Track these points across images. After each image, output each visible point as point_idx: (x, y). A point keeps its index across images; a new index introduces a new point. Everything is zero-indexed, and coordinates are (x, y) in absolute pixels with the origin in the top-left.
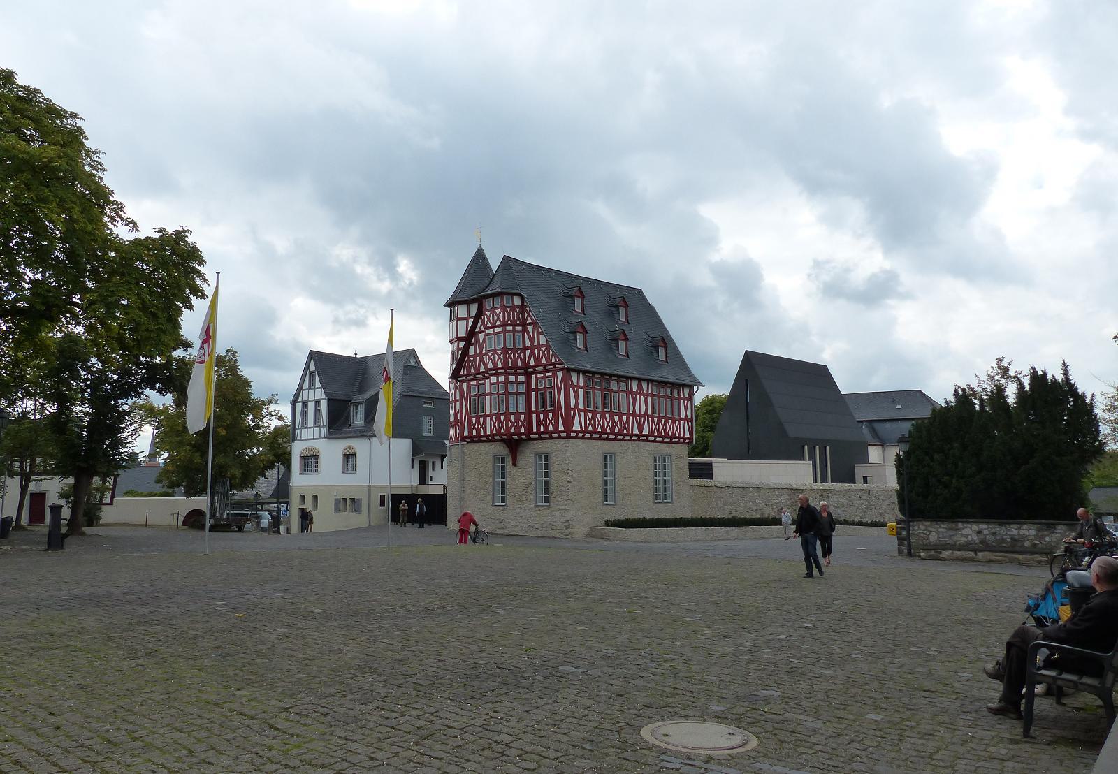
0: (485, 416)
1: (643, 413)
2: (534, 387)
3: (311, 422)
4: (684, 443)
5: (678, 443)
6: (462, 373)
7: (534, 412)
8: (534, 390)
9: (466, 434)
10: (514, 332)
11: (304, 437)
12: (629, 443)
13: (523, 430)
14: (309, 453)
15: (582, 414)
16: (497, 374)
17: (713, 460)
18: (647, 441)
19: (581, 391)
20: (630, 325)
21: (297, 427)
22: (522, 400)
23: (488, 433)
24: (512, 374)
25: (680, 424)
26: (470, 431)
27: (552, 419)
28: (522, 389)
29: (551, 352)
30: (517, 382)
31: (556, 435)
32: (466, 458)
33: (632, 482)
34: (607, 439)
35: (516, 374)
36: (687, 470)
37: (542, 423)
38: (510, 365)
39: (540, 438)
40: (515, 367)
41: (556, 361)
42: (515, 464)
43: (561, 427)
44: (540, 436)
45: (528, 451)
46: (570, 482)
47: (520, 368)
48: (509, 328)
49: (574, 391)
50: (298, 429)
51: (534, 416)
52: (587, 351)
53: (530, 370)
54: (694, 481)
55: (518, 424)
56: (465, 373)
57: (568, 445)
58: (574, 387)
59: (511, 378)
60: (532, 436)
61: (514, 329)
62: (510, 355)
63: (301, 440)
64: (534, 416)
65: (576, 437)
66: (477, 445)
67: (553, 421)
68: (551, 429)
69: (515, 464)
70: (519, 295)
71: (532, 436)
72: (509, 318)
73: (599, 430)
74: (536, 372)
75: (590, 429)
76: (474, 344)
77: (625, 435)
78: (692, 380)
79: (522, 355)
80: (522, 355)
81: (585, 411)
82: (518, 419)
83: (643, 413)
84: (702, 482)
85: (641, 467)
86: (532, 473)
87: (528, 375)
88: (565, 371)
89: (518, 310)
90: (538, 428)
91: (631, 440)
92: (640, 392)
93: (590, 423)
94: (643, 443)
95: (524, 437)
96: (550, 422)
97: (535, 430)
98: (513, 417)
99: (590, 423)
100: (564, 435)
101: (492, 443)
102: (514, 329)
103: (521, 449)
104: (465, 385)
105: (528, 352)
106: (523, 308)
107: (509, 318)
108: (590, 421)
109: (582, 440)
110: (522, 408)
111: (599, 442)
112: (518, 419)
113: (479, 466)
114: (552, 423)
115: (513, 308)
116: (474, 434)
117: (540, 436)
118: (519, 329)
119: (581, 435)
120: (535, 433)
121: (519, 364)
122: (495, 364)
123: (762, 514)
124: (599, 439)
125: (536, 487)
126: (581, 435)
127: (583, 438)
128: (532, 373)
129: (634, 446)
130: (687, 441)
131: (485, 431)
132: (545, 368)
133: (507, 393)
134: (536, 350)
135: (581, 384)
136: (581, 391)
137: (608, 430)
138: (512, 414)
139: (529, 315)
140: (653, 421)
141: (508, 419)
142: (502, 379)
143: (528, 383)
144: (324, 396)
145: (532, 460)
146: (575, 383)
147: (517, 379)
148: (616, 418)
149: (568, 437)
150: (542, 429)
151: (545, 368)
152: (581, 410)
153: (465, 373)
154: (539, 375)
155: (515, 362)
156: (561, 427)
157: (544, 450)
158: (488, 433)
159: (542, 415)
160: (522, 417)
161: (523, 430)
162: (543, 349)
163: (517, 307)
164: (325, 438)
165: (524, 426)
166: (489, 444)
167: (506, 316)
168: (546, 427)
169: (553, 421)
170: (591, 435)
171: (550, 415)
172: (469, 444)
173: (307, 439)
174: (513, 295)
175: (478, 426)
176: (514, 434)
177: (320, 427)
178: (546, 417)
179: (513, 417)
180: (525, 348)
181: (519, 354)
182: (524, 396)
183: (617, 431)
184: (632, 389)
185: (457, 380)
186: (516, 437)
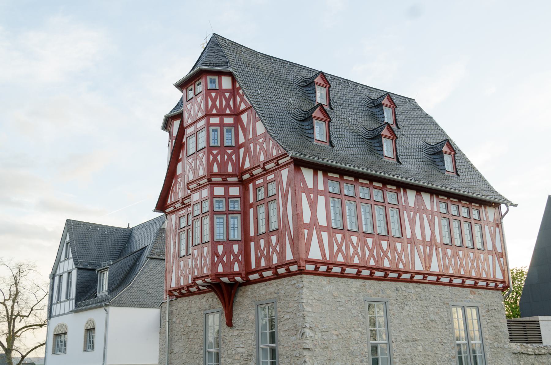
1: (428, 239)
2: (251, 201)
3: (63, 297)
4: (496, 288)
5: (486, 288)
6: (169, 202)
8: (251, 206)
10: (222, 125)
11: (58, 313)
12: (410, 285)
13: (236, 268)
14: (60, 330)
15: (325, 235)
17: (540, 318)
18: (437, 283)
19: (321, 200)
20: (400, 130)
21: (53, 302)
22: (236, 223)
24: (218, 184)
25: (486, 260)
28: (236, 206)
29: (271, 143)
30: (227, 197)
32: (174, 320)
33: (420, 348)
34: (371, 277)
35: (225, 184)
36: (506, 330)
38: (215, 170)
39: (262, 280)
40: (224, 175)
41: (277, 151)
42: (230, 324)
44: (261, 275)
45: (247, 301)
46: (309, 349)
47: (231, 175)
48: (215, 120)
49: (308, 197)
50: (54, 304)
51: (252, 244)
52: (332, 146)
53: (246, 176)
54: (516, 347)
55: (228, 258)
56: (173, 200)
57: (301, 285)
58: (308, 191)
59: (219, 191)
60: (253, 277)
61: (222, 120)
62: (215, 156)
63: (56, 316)
65: (316, 273)
66: (187, 299)
67: (278, 248)
69: (230, 324)
70: (229, 74)
71: (253, 277)
72: (214, 106)
73: (356, 261)
74: (253, 178)
75: (340, 259)
77: (400, 272)
78: (497, 197)
79: (233, 157)
80: (233, 157)
81: (332, 231)
82: (228, 251)
83: (428, 239)
84: (530, 348)
85: (434, 324)
86: (253, 337)
87: (243, 184)
88: (292, 166)
89: (227, 95)
90: (258, 261)
91: (411, 280)
92: (420, 209)
93: (340, 250)
94: (433, 287)
95: (238, 279)
96: (275, 250)
97: (253, 266)
98: (220, 249)
99: (340, 250)
100: (294, 268)
101: (203, 295)
102: (222, 120)
103: (238, 299)
104: (173, 217)
105: (242, 151)
106: (234, 91)
107: (214, 106)
108: (340, 246)
109: (327, 279)
110: (236, 234)
111: (358, 283)
112: (228, 251)
113: (189, 330)
115: (220, 92)
117: (261, 275)
118: (229, 120)
119: (323, 268)
121: (230, 169)
122: (195, 172)
124: (358, 276)
125: (258, 360)
126: (323, 268)
127: (328, 274)
129: (419, 290)
130: (501, 286)
132: (264, 169)
133: (214, 213)
134: (252, 145)
135: (321, 187)
136: (321, 200)
137: (372, 263)
138: (219, 242)
139: (242, 100)
140: (445, 254)
141: (214, 253)
142: (205, 193)
143: (244, 196)
144: (74, 267)
145: (252, 317)
146: (310, 185)
147: (227, 191)
148: (384, 244)
149: (301, 272)
150: (263, 264)
151: (264, 169)
152: (321, 229)
153: (173, 200)
155: (223, 165)
157: (268, 297)
159: (262, 242)
160: (236, 248)
161: (236, 268)
162: (261, 141)
163: (227, 91)
164: (71, 312)
165: (239, 262)
166: (200, 296)
167: (210, 103)
168: (269, 259)
169: (278, 248)
170: (343, 270)
171: (274, 239)
172: (179, 299)
173: (60, 315)
174: (220, 74)
176: (223, 275)
177: (69, 300)
178: (268, 243)
179: (220, 249)
180: (239, 146)
181: (230, 156)
182: (239, 216)
183: (386, 264)
184: (406, 201)
185: (165, 213)
186: (225, 279)
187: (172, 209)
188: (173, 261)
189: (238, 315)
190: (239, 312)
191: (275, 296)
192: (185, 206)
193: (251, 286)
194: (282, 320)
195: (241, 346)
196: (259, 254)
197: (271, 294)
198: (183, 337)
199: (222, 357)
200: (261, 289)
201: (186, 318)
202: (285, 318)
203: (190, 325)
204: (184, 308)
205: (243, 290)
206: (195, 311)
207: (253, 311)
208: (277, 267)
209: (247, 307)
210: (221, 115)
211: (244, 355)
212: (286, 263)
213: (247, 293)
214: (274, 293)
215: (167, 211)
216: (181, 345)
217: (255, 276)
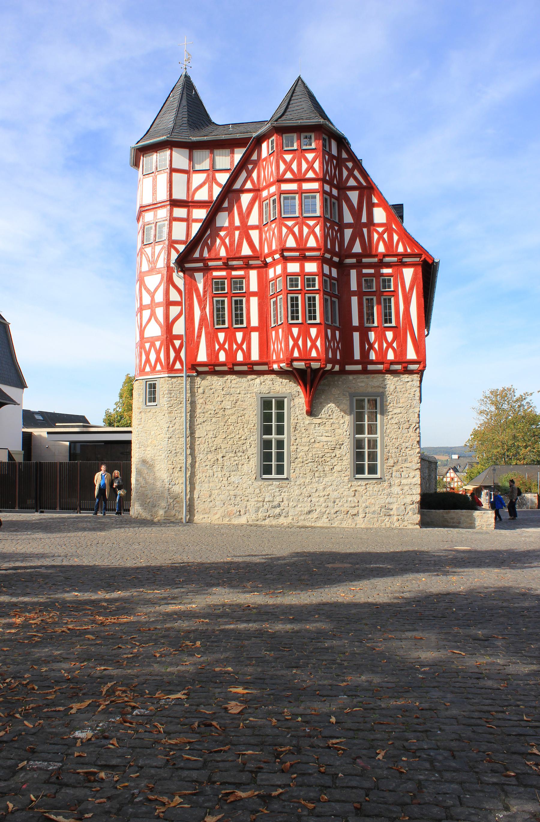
0: (247, 331)
6: (197, 255)
7: (356, 329)
8: (354, 293)
9: (202, 356)
16: (303, 259)
23: (255, 356)
26: (212, 353)
27: (393, 341)
31: (399, 367)
37: (371, 346)
39: (365, 371)
43: (411, 354)
51: (356, 336)
56: (206, 254)
64: (356, 336)
67: (395, 345)
68: (391, 356)
71: (348, 368)
74: (359, 266)
76: (230, 210)
90: (365, 354)
97: (357, 356)
105: (348, 233)
114: (393, 349)
116: (222, 357)
120: (357, 363)
123: (418, 502)
128: (352, 266)
131: (247, 354)
150: (373, 356)
154: (365, 271)
156: (411, 354)
158: (255, 356)
171: (390, 335)
175: (231, 346)
187: (201, 265)
188: (200, 329)
189: (321, 403)
190: (322, 400)
191: (381, 390)
192: (227, 267)
193: (344, 377)
194: (390, 413)
195: (327, 434)
196: (367, 346)
197: (374, 387)
198: (214, 420)
199: (293, 445)
200: (358, 380)
201: (219, 399)
202: (395, 411)
203: (229, 407)
204: (212, 387)
205: (336, 378)
206: (238, 392)
207: (348, 403)
208: (392, 363)
209: (336, 396)
210: (300, 179)
211: (329, 443)
212: (404, 360)
213: (336, 383)
214: (379, 387)
215: (187, 265)
216: (208, 428)
217: (359, 367)
